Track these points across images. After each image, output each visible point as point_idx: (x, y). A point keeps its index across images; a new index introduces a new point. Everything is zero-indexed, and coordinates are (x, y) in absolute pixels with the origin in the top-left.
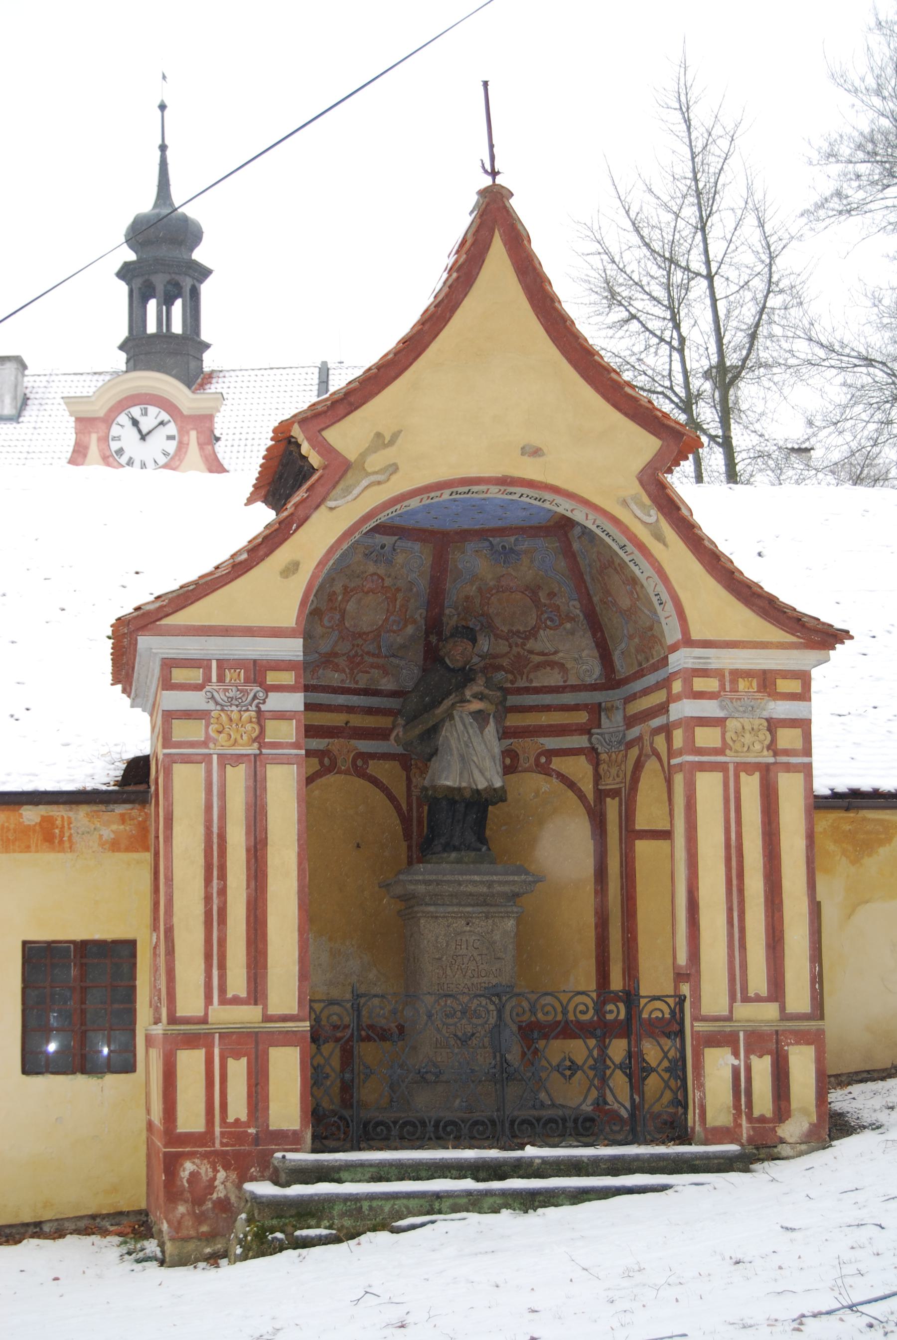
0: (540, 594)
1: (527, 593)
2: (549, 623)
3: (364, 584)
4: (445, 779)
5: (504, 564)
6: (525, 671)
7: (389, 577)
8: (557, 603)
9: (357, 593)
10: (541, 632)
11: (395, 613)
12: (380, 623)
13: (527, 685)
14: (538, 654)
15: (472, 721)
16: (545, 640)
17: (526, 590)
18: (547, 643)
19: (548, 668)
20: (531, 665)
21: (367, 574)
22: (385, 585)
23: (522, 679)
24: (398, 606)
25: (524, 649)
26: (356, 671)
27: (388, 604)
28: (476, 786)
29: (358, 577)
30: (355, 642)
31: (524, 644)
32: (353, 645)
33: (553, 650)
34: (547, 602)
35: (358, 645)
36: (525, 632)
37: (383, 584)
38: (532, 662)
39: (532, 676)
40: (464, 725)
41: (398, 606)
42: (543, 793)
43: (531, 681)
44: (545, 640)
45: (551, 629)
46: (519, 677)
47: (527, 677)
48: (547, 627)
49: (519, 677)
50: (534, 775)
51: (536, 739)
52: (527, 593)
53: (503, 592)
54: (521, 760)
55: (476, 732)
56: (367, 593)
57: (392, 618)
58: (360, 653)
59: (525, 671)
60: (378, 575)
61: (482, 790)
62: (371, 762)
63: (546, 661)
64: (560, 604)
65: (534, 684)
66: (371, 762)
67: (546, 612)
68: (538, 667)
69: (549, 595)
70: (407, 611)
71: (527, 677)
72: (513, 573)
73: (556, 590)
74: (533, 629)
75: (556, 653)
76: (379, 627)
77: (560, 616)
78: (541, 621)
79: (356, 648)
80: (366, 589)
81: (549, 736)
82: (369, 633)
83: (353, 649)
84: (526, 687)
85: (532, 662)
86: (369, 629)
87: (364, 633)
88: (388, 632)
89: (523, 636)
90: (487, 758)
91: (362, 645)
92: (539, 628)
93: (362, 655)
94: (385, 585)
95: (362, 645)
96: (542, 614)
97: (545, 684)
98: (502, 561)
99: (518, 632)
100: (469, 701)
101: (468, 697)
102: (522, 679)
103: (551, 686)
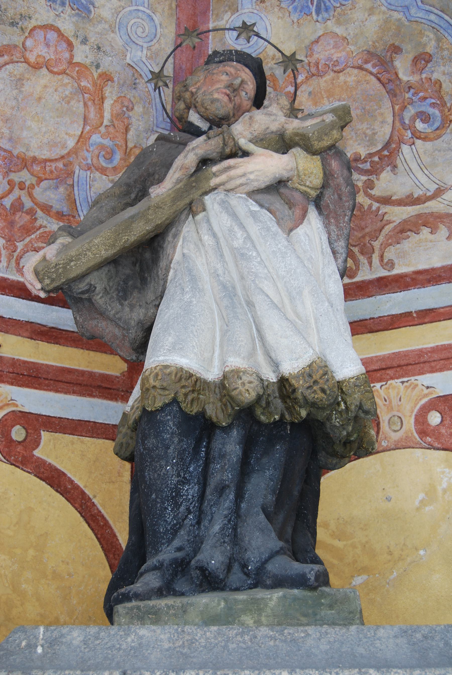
0: (398, 63)
1: (369, 66)
2: (420, 126)
3: (29, 43)
4: (173, 348)
5: (318, 12)
6: (376, 244)
7: (85, 41)
8: (435, 76)
9: (12, 62)
10: (405, 148)
11: (102, 129)
12: (71, 143)
13: (383, 273)
14: (401, 203)
15: (256, 208)
16: (414, 166)
17: (366, 62)
18: (420, 175)
19: (425, 231)
20: (388, 228)
21: (33, 23)
22: (77, 59)
23: (370, 263)
24: (107, 115)
25: (371, 197)
26: (20, 246)
27: (85, 105)
28: (276, 365)
29: (13, 24)
30: (16, 177)
31: (370, 185)
32: (11, 183)
33: (433, 188)
34: (414, 79)
35: (22, 186)
36: (371, 155)
37: (72, 57)
38: (389, 222)
39: (390, 254)
40: (234, 215)
41: (107, 115)
42: (445, 491)
43: (391, 265)
44: (414, 166)
45: (425, 139)
46: (363, 259)
47: (382, 257)
48: (417, 135)
49: (363, 259)
50: (418, 452)
51: (413, 378)
52: (369, 66)
53: (319, 74)
54: (384, 426)
55: (268, 229)
56: (36, 67)
57: (96, 138)
58: (28, 204)
59: (376, 244)
60: (57, 30)
61: (296, 377)
62: (45, 435)
63: (419, 216)
64: (442, 79)
65: (396, 271)
66: (45, 435)
67: (411, 102)
68: (402, 231)
69: (416, 60)
70: (127, 130)
71: (382, 257)
72: (339, 31)
73: (430, 48)
74: (387, 146)
75: (439, 193)
76: (69, 154)
77: (444, 104)
78: (403, 123)
79: (17, 192)
80: (32, 58)
81: (441, 370)
82: (46, 161)
83: (10, 191)
84: (380, 279)
85: (389, 222)
86: (45, 154)
87: (34, 159)
88: (89, 168)
89: (367, 166)
90: (306, 292)
91: (32, 187)
92: (401, 141)
93: (31, 212)
94: (77, 59)
95: (32, 187)
96: (404, 108)
97: (421, 267)
98: (313, 9)
99: (357, 159)
100: (246, 154)
101: (243, 142)
102: (370, 263)
103: (433, 269)
